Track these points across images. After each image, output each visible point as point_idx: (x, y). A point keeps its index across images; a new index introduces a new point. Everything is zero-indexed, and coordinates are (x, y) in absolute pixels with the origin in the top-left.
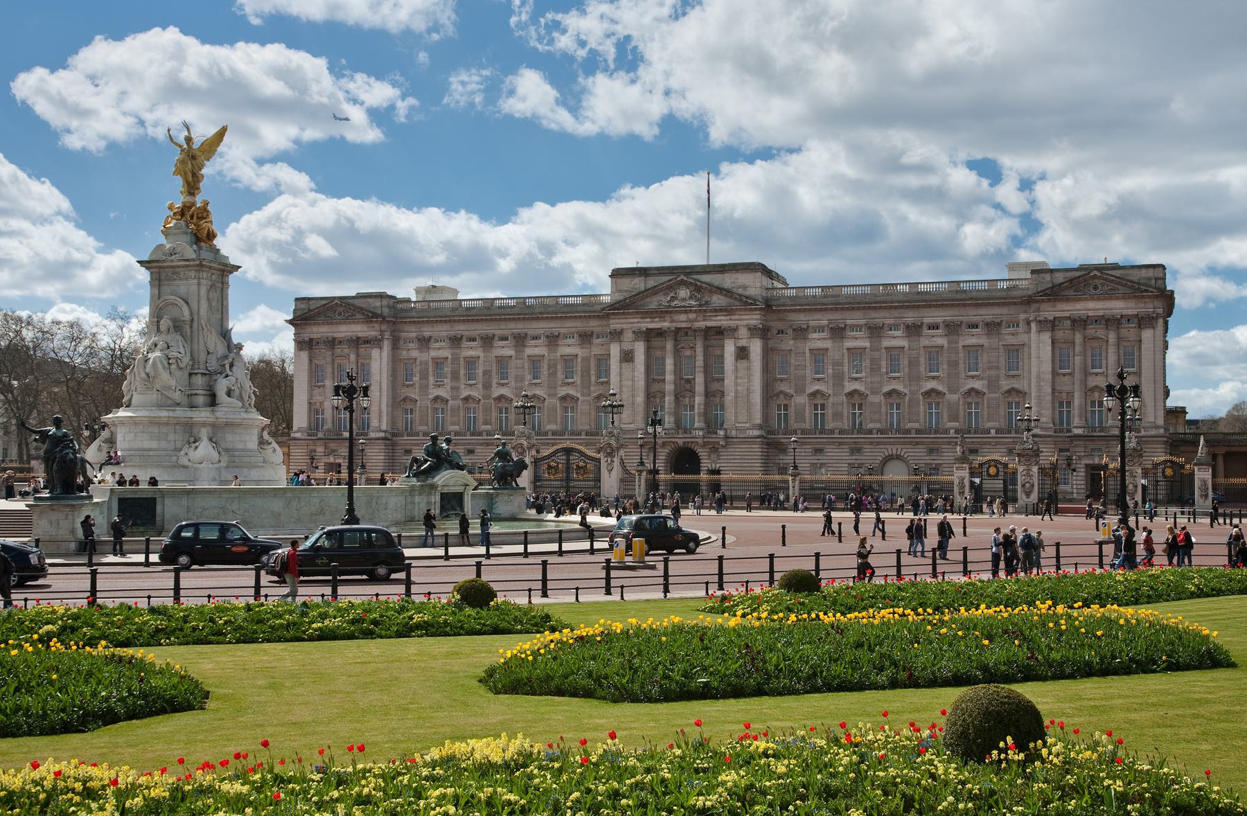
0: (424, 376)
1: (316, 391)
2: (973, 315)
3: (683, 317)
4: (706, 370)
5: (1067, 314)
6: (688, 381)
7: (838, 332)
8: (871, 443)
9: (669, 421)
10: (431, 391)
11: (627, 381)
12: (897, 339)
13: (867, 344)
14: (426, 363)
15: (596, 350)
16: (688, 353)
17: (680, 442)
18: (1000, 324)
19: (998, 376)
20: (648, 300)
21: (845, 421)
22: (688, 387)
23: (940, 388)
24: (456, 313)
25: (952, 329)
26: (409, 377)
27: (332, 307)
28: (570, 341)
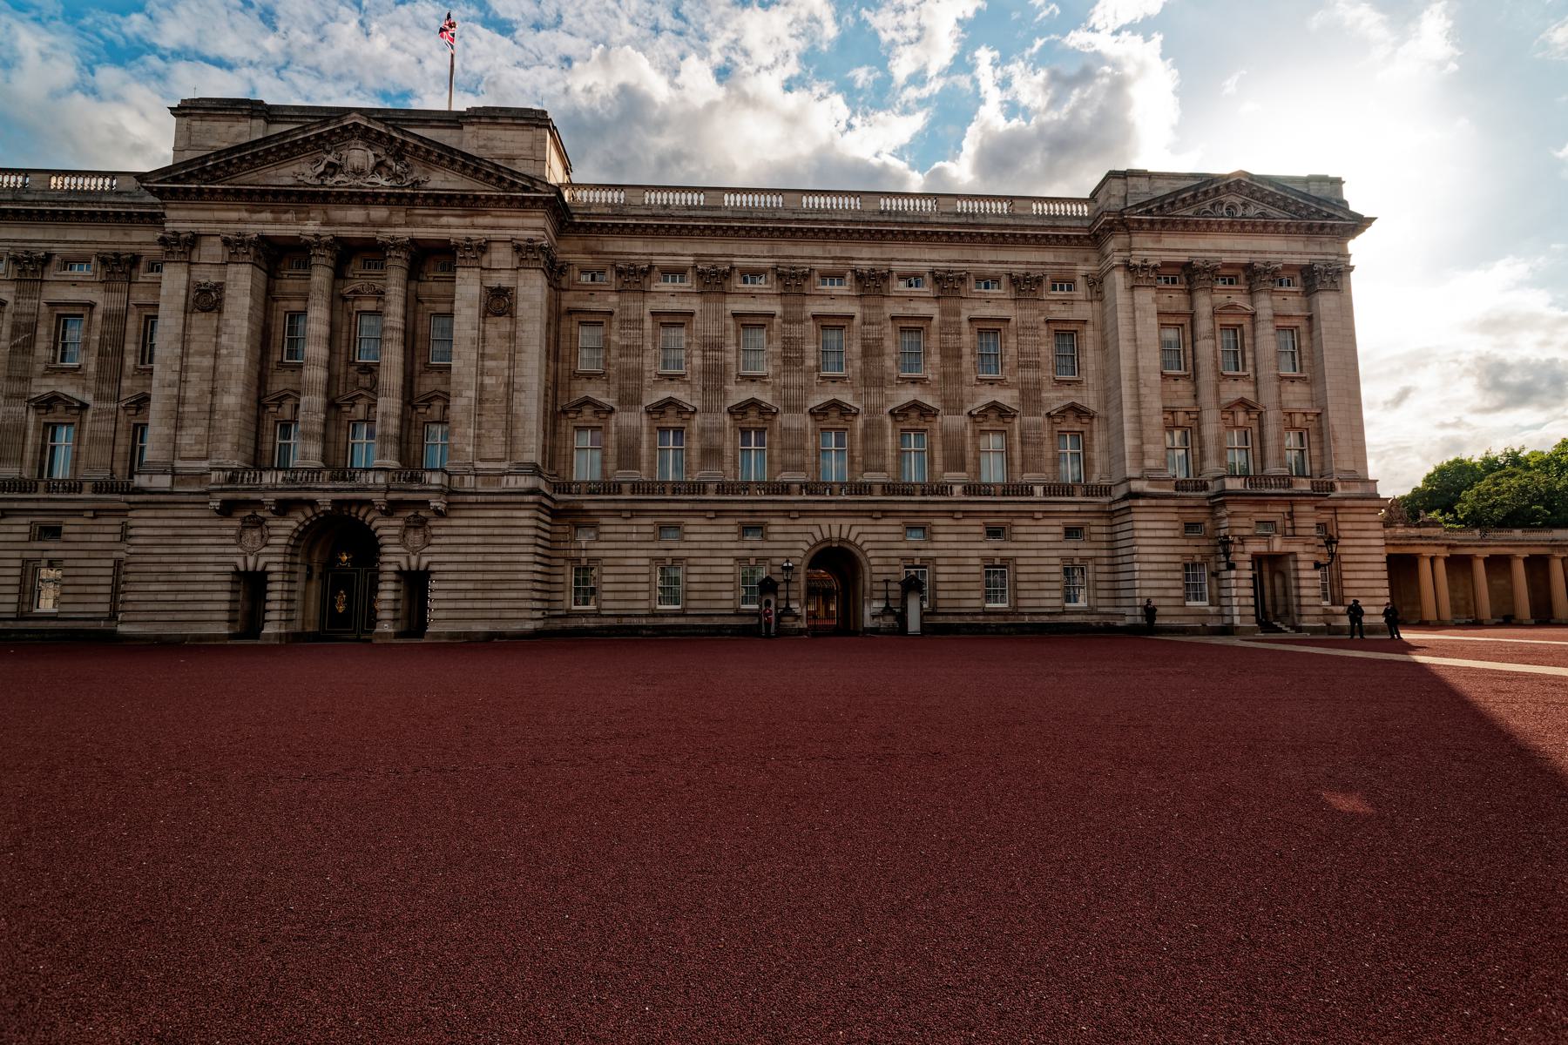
2: (988, 259)
3: (356, 214)
4: (411, 340)
5: (1183, 258)
7: (714, 281)
8: (787, 514)
9: (306, 452)
11: (201, 359)
13: (777, 309)
15: (140, 296)
17: (325, 500)
18: (1039, 281)
19: (1038, 382)
21: (728, 466)
22: (365, 380)
23: (929, 401)
25: (947, 284)
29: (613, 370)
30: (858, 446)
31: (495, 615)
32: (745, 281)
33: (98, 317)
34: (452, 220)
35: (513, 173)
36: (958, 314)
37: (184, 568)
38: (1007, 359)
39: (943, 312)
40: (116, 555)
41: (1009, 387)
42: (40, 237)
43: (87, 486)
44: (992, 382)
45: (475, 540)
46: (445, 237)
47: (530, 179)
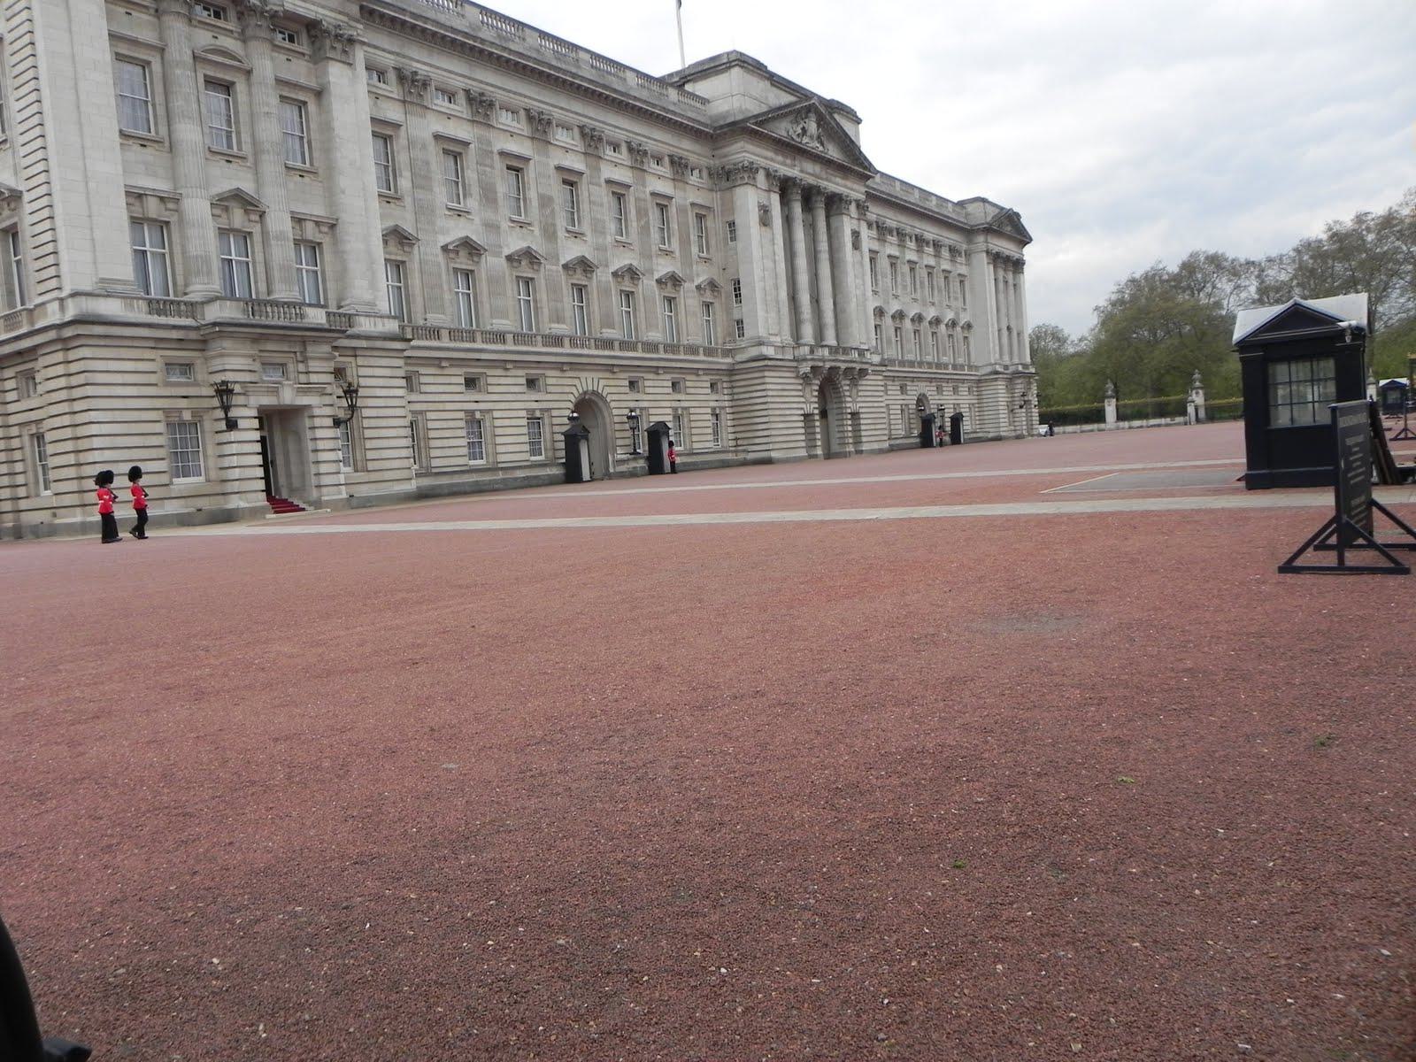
0: (421, 180)
3: (810, 167)
5: (996, 249)
20: (777, 124)
28: (660, 170)
31: (877, 438)
33: (674, 210)
34: (838, 180)
37: (788, 412)
43: (701, 350)
44: (949, 307)
45: (869, 393)
46: (837, 191)
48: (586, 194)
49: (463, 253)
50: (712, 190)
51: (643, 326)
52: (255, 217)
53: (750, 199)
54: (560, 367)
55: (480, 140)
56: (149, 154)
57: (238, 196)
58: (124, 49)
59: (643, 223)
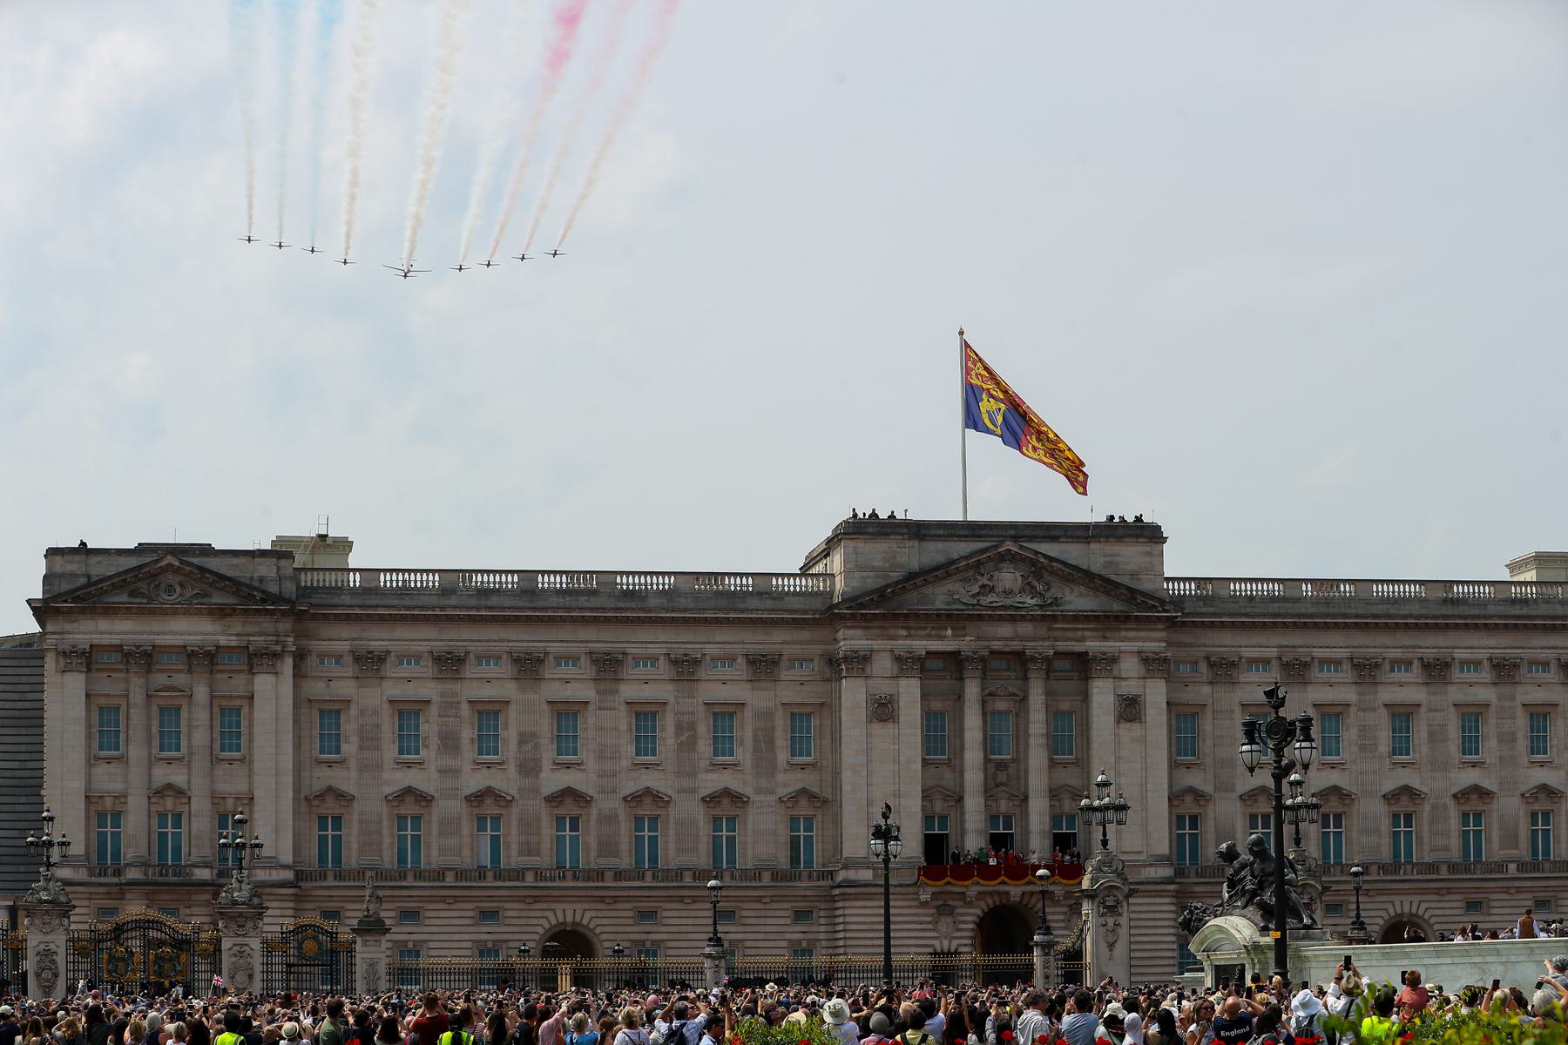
0: (369, 741)
1: (101, 770)
3: (1005, 630)
6: (1002, 766)
10: (385, 776)
12: (1405, 688)
14: (375, 712)
16: (1001, 705)
20: (928, 590)
22: (1002, 777)
23: (1486, 784)
24: (453, 601)
25: (1504, 670)
26: (332, 741)
27: (154, 576)
28: (726, 672)
29: (1208, 760)
30: (1426, 827)
32: (1321, 671)
35: (1144, 594)
36: (1513, 698)
38: (1555, 742)
39: (1500, 697)
40: (788, 936)
41: (1556, 768)
42: (692, 638)
43: (766, 876)
44: (1542, 765)
47: (1162, 602)
48: (591, 721)
49: (409, 799)
50: (828, 680)
51: (671, 853)
52: (184, 800)
53: (853, 695)
54: (522, 900)
55: (442, 694)
56: (113, 768)
57: (169, 786)
58: (102, 701)
59: (683, 738)
